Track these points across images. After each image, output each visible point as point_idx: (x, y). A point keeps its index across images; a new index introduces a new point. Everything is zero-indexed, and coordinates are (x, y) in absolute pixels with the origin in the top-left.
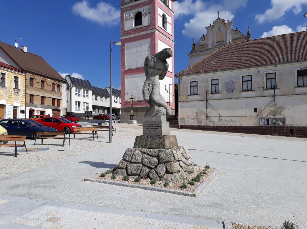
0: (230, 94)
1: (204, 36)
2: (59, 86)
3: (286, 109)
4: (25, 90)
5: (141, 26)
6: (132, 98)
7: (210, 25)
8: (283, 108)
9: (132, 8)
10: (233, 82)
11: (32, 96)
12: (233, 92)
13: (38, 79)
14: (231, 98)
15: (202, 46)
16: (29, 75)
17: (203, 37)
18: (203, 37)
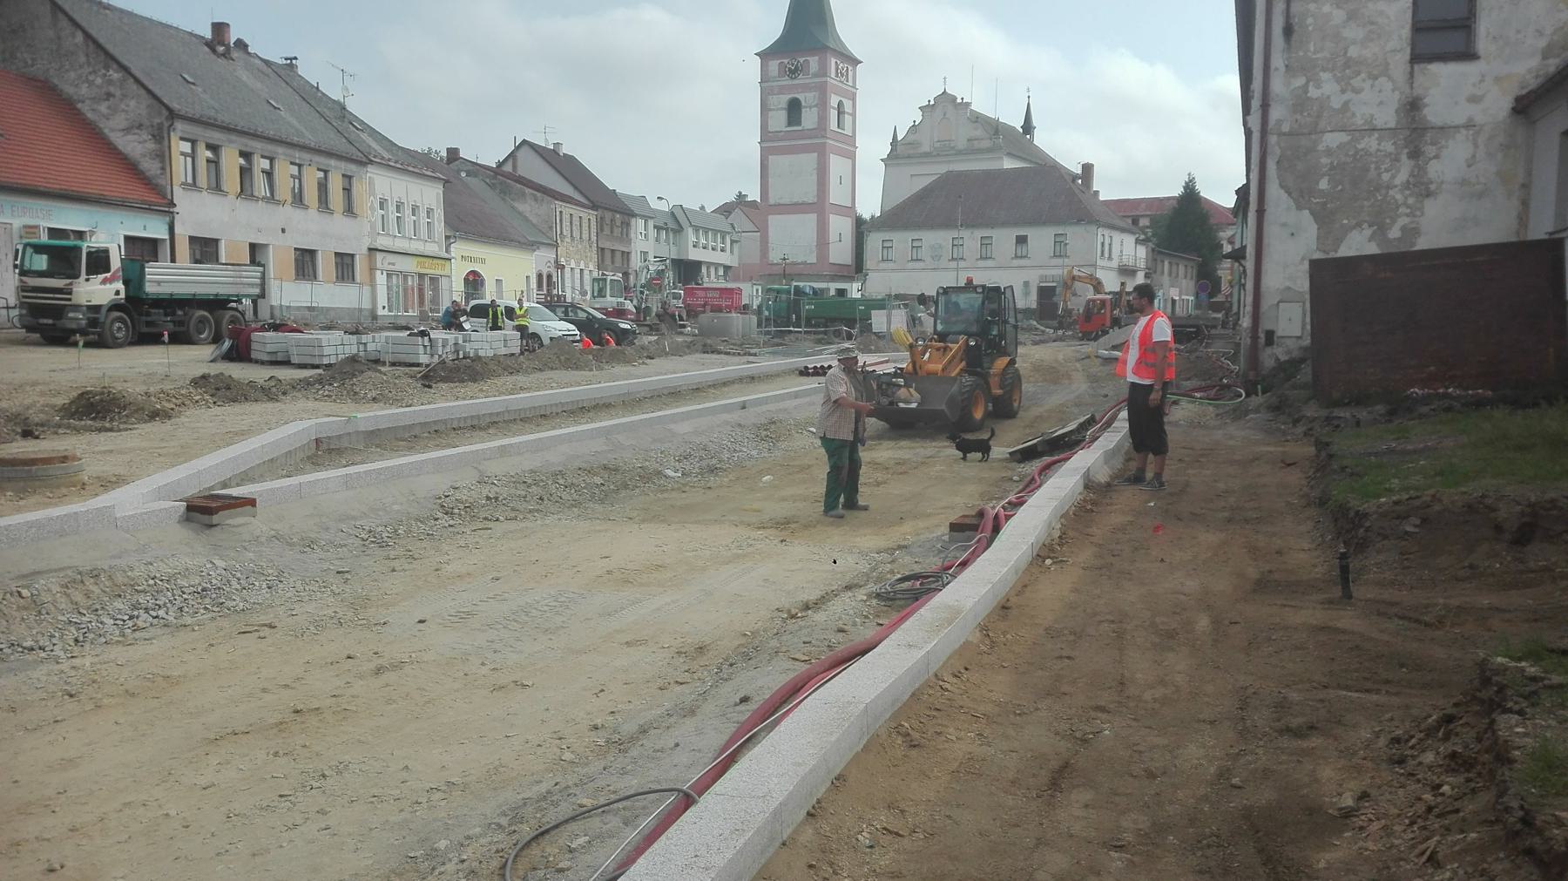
2: (628, 225)
4: (597, 241)
5: (800, 128)
6: (784, 259)
9: (782, 90)
10: (941, 247)
11: (603, 249)
12: (939, 260)
13: (608, 215)
16: (600, 212)
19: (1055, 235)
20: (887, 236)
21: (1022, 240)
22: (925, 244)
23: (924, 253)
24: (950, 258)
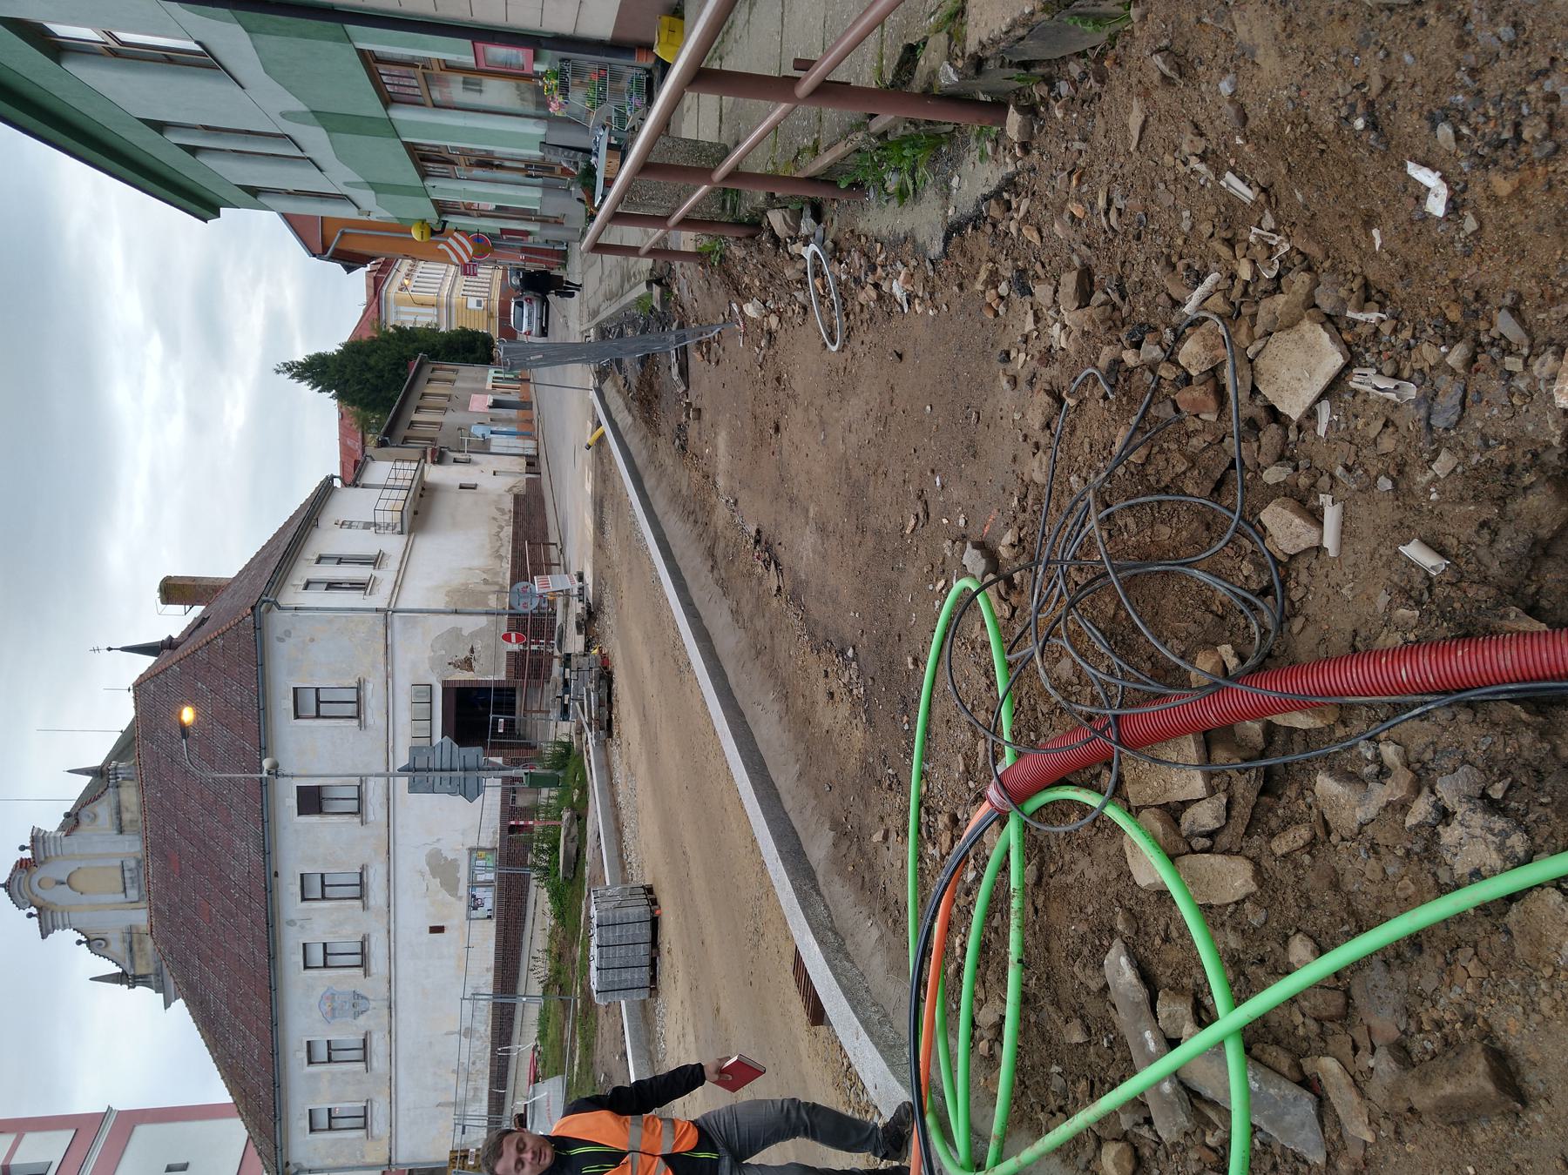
0: (373, 1004)
1: (83, 939)
3: (437, 846)
7: (35, 920)
12: (363, 998)
14: (387, 1003)
15: (136, 947)
17: (88, 943)
18: (89, 946)
19: (297, 717)
20: (298, 1123)
21: (312, 801)
22: (322, 1035)
23: (346, 1033)
24: (360, 971)
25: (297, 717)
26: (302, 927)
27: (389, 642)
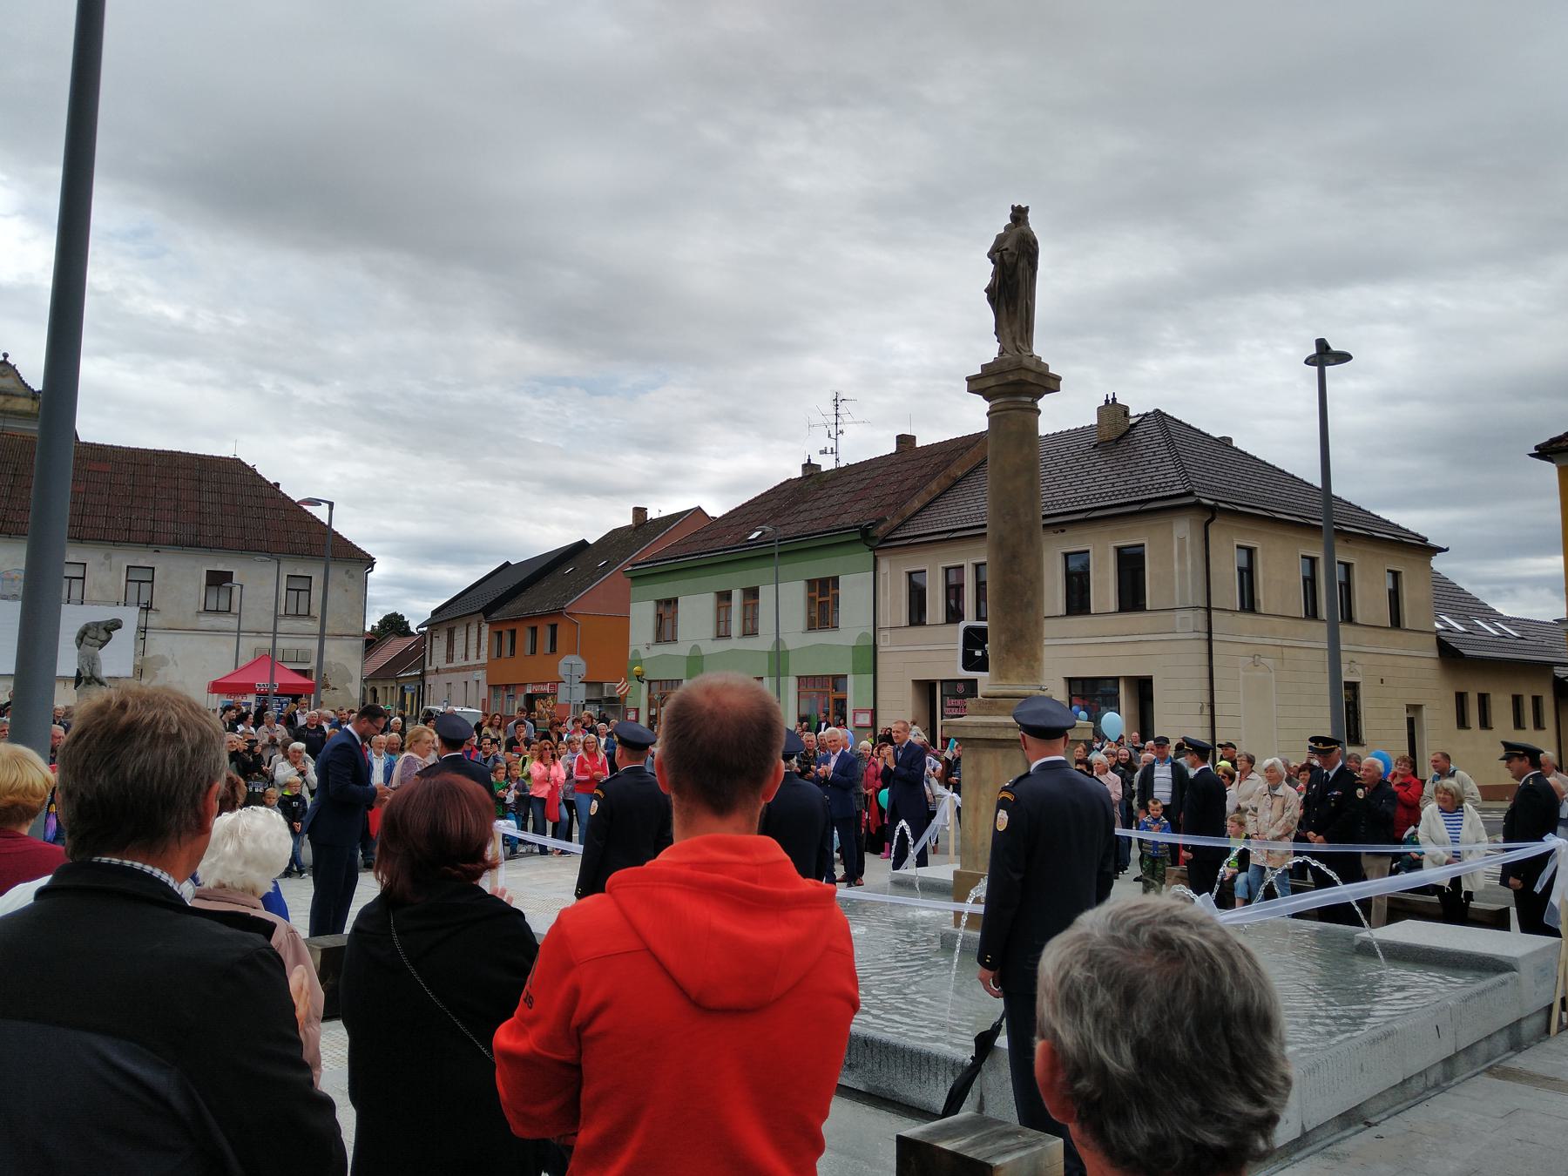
3: (171, 663)
8: (163, 661)
19: (288, 576)
21: (218, 580)
25: (288, 576)
26: (103, 564)
27: (344, 637)
